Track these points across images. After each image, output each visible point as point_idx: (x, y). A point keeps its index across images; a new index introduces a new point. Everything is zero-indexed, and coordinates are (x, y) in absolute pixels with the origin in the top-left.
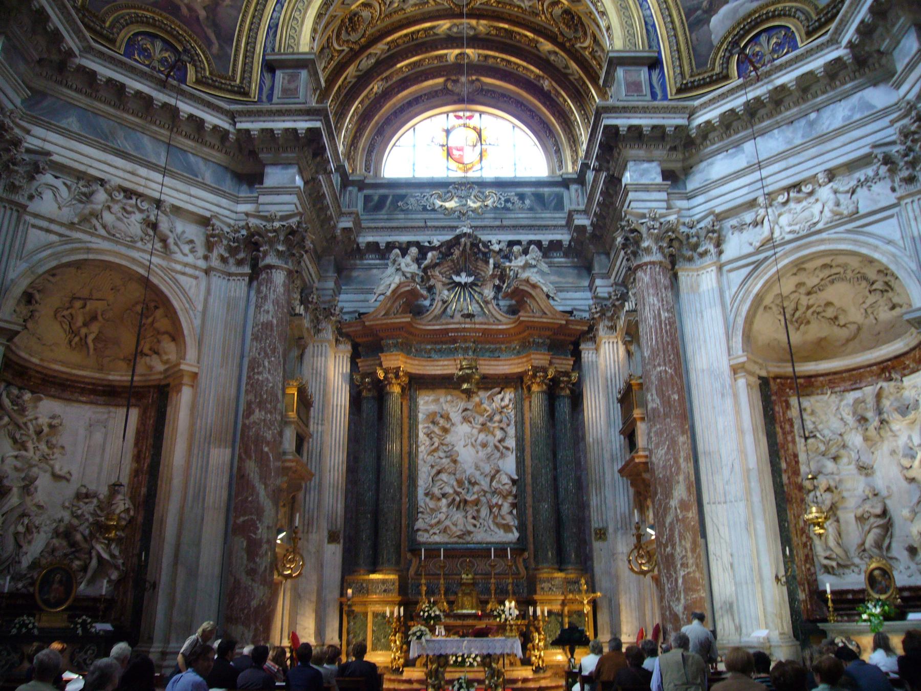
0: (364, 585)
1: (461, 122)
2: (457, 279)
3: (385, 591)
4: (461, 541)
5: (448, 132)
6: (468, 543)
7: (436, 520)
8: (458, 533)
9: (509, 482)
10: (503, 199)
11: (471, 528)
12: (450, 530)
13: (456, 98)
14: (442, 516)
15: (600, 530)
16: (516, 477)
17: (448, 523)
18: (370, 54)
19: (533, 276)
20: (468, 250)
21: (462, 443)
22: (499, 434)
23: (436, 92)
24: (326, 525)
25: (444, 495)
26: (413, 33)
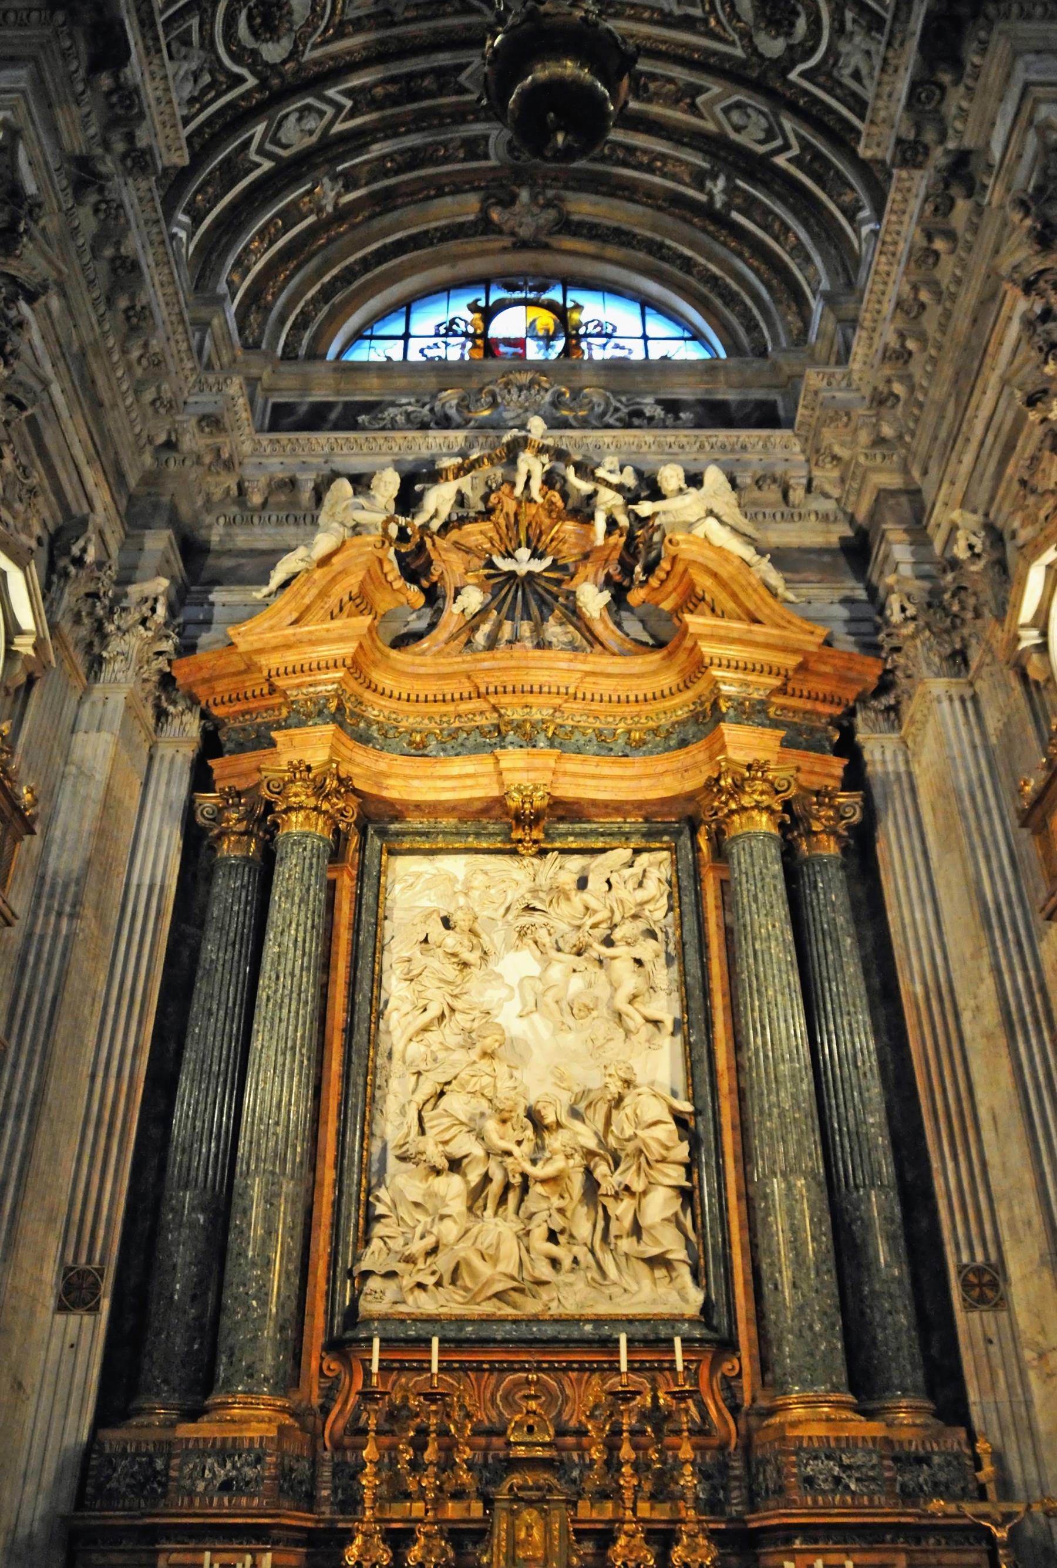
0: (159, 1464)
1: (518, 295)
2: (504, 565)
3: (226, 1486)
4: (508, 1311)
5: (488, 314)
6: (535, 1320)
7: (430, 1241)
8: (499, 1287)
9: (670, 1119)
10: (625, 410)
11: (544, 1271)
12: (474, 1274)
13: (507, 241)
14: (449, 1231)
15: (979, 1271)
16: (686, 1107)
17: (465, 1251)
18: (308, 108)
19: (721, 536)
20: (535, 493)
21: (515, 1006)
22: (630, 981)
23: (462, 225)
24: (53, 1247)
25: (455, 1165)
26: (410, 76)
